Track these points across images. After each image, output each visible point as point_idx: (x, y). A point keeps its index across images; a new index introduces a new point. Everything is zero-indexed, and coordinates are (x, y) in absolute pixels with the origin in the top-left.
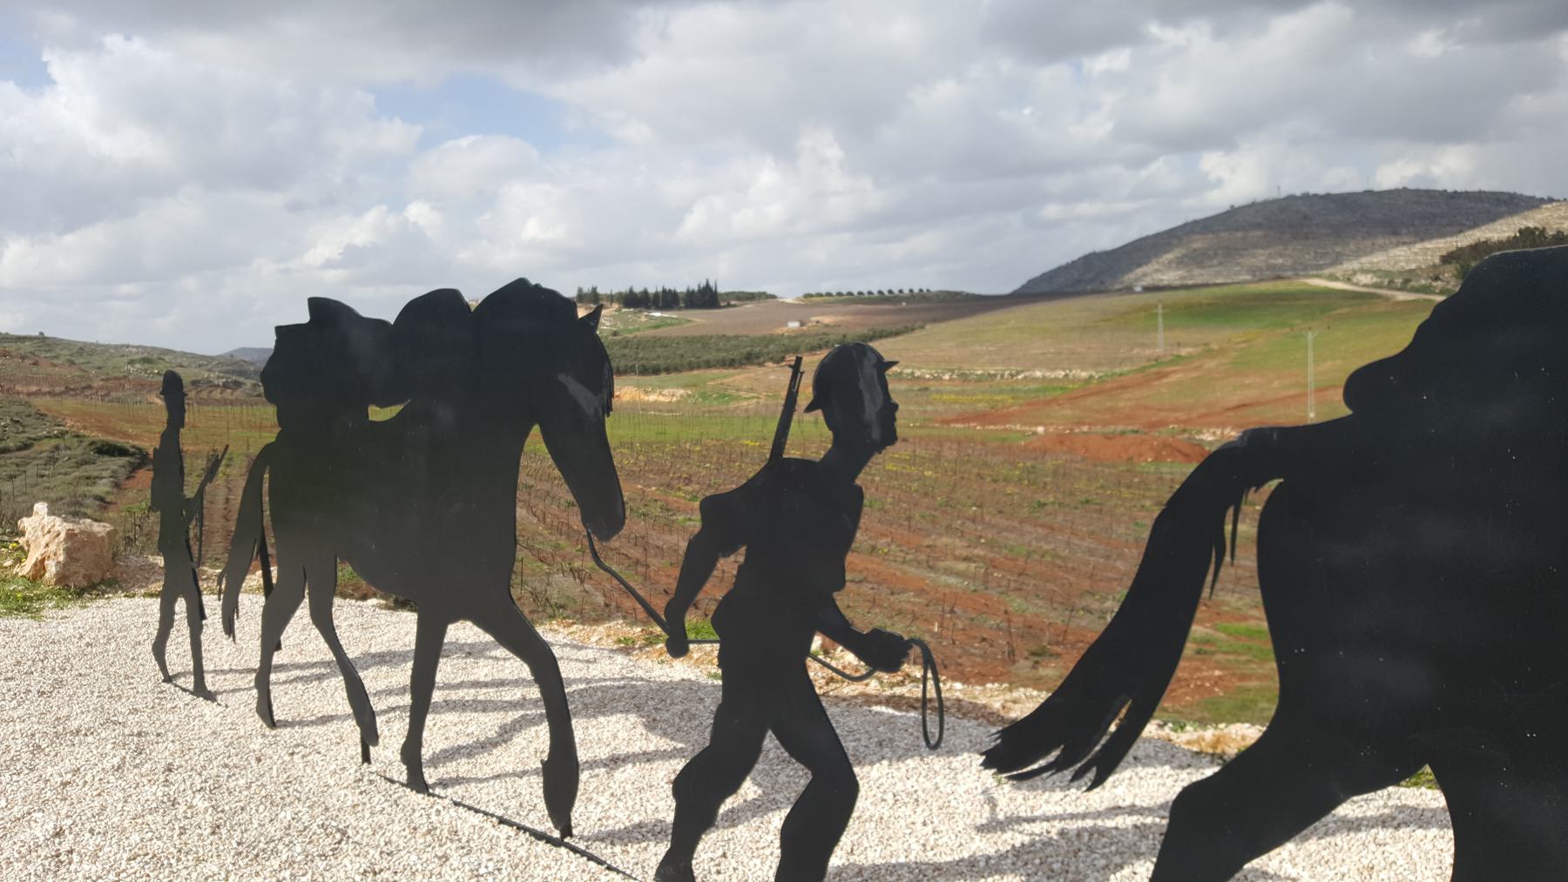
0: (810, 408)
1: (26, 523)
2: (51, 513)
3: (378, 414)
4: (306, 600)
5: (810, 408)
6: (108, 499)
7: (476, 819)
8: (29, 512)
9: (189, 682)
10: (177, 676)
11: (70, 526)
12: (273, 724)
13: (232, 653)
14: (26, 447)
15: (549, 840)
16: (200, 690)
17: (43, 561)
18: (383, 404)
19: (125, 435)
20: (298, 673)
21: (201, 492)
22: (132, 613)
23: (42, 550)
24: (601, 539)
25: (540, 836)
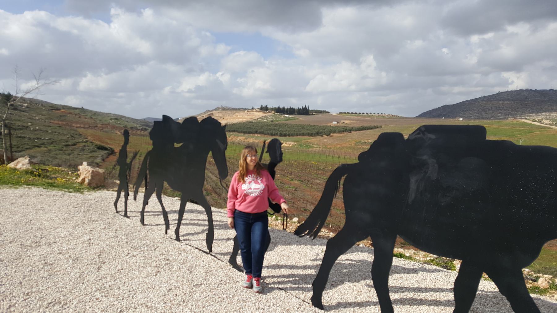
0: (267, 152)
2: (89, 165)
3: (177, 145)
5: (267, 152)
6: (100, 164)
7: (190, 247)
9: (123, 213)
11: (93, 169)
13: (135, 205)
14: (75, 145)
15: (206, 253)
16: (126, 215)
18: (178, 143)
20: (152, 213)
21: (131, 162)
22: (110, 195)
25: (204, 252)
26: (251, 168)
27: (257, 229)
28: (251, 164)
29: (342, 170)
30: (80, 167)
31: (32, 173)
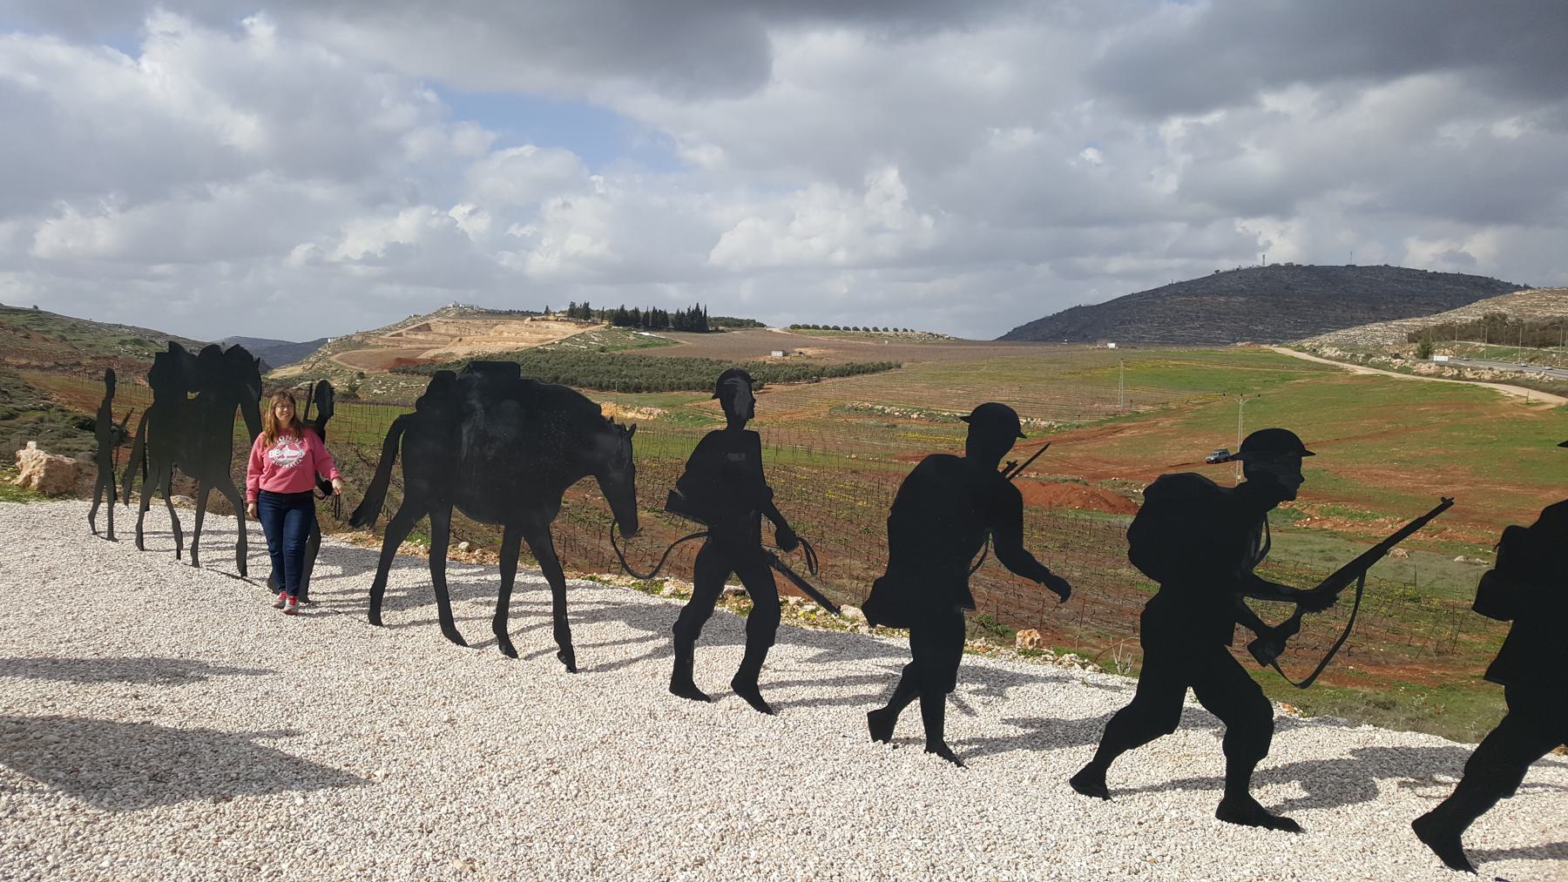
1: (22, 453)
3: (191, 395)
8: (24, 446)
12: (142, 549)
14: (11, 416)
26: (285, 424)
27: (293, 520)
28: (281, 419)
29: (400, 424)
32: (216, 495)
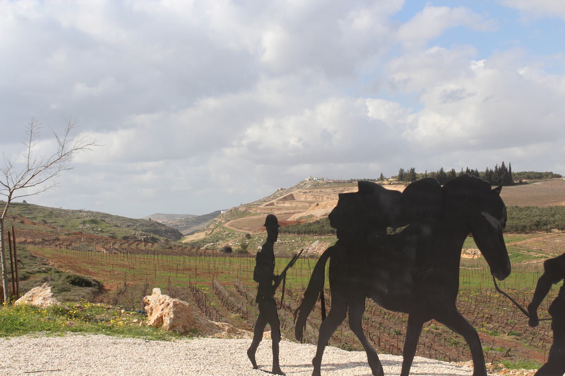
4: (347, 318)
10: (260, 366)
17: (162, 317)
19: (87, 272)
21: (284, 273)
23: (160, 312)
24: (500, 279)
30: (149, 297)
31: (63, 312)
32: (345, 331)
